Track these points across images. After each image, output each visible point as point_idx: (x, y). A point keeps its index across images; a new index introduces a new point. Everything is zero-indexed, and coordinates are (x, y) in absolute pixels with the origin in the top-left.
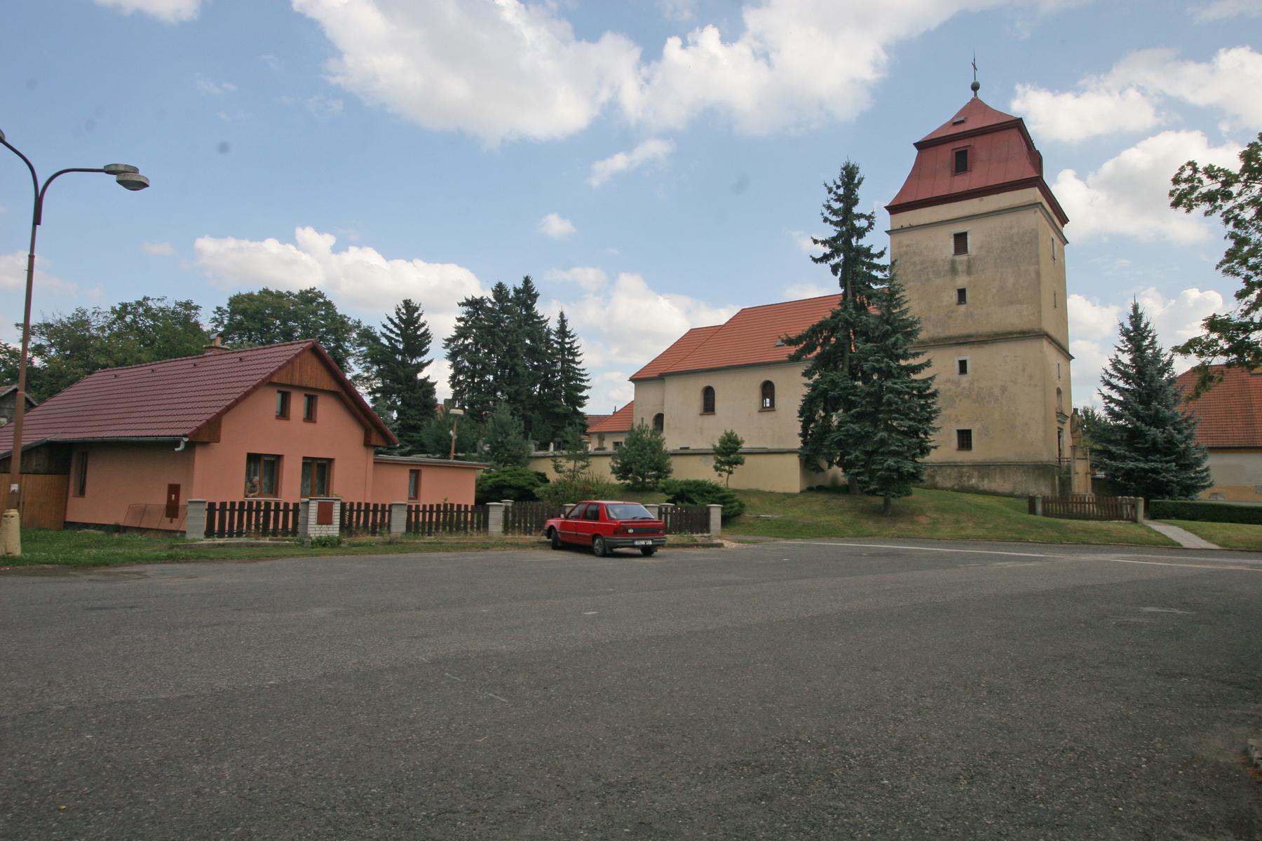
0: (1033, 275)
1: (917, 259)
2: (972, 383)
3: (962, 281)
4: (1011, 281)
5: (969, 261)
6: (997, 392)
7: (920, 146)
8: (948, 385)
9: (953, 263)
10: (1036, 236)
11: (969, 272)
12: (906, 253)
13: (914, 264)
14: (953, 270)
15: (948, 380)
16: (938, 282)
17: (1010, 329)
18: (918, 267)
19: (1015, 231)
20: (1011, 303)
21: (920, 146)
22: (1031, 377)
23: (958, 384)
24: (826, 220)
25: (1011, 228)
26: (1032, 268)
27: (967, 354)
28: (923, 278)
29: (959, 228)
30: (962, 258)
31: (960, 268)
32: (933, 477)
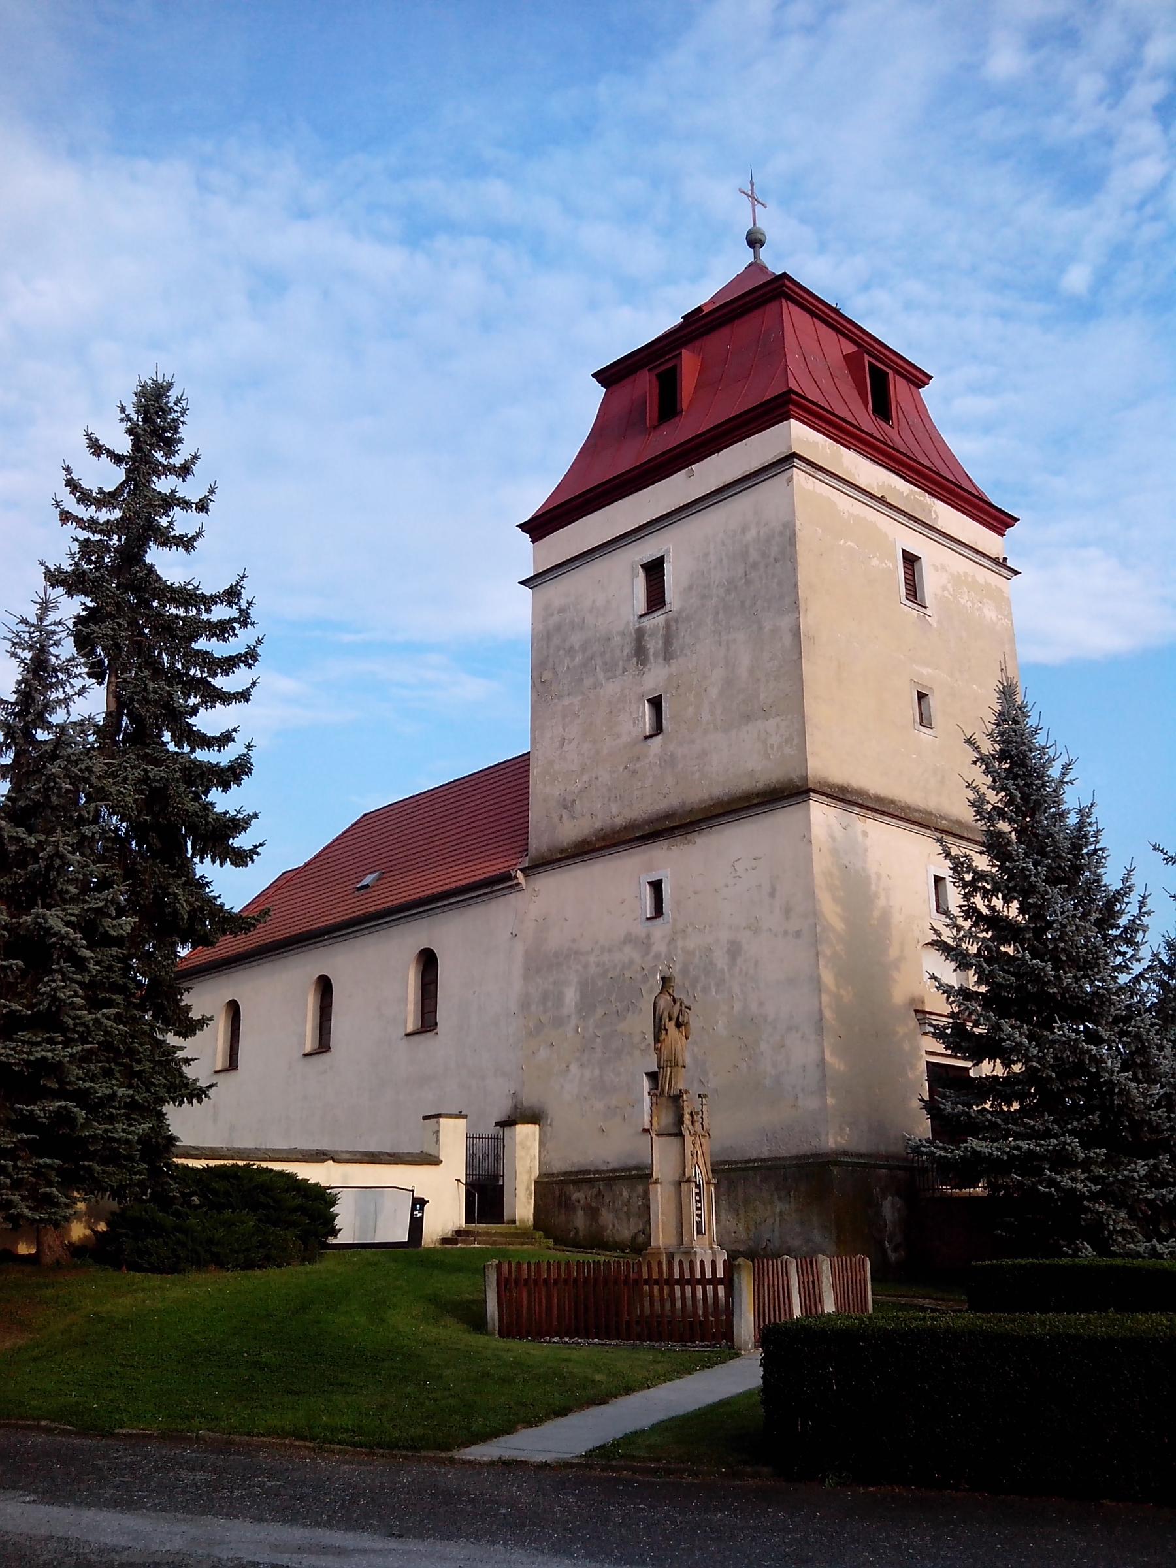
0: (788, 640)
1: (576, 639)
2: (672, 941)
3: (655, 678)
4: (745, 661)
5: (667, 626)
6: (721, 960)
7: (607, 377)
8: (628, 949)
9: (640, 634)
10: (792, 541)
11: (668, 655)
12: (558, 628)
13: (571, 651)
14: (640, 653)
15: (629, 939)
16: (611, 689)
17: (745, 785)
18: (579, 658)
19: (752, 534)
20: (747, 718)
21: (602, 376)
22: (787, 911)
23: (645, 944)
24: (66, 517)
25: (744, 530)
26: (785, 622)
27: (666, 861)
28: (588, 682)
29: (647, 550)
30: (658, 619)
31: (653, 645)
32: (593, 1213)
